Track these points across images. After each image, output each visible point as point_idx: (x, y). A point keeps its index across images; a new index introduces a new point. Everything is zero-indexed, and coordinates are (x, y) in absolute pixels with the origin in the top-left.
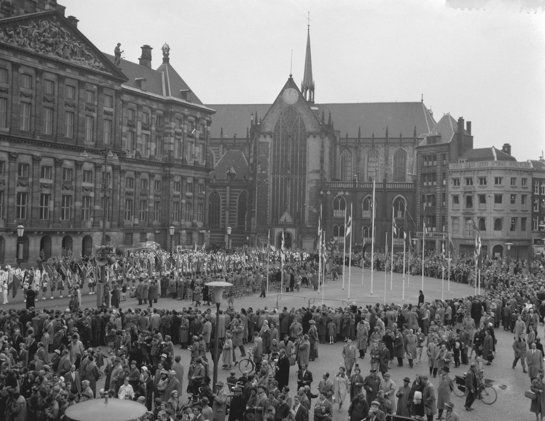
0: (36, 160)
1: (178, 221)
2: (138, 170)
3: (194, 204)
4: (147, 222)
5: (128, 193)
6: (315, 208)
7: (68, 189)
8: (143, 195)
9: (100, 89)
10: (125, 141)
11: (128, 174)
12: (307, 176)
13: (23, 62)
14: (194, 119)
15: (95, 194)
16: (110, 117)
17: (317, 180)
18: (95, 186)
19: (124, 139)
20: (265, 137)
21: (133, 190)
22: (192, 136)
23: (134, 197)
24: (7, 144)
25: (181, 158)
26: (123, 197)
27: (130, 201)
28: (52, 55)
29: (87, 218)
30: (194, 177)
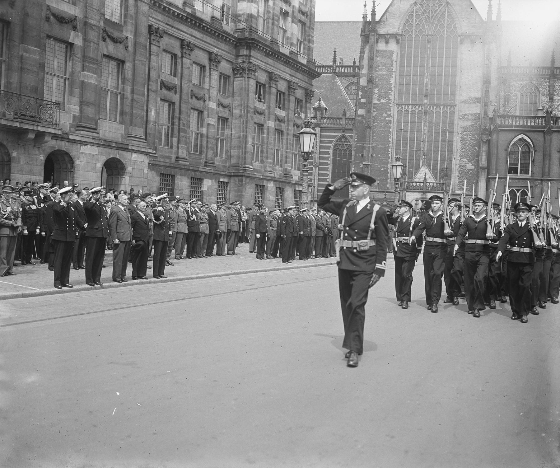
1: (262, 162)
2: (188, 38)
3: (288, 134)
4: (204, 155)
6: (470, 161)
11: (166, 40)
12: (457, 108)
15: (85, 40)
17: (475, 114)
18: (86, 17)
20: (387, 42)
21: (176, 81)
23: (178, 96)
25: (269, 38)
26: (156, 91)
30: (289, 82)
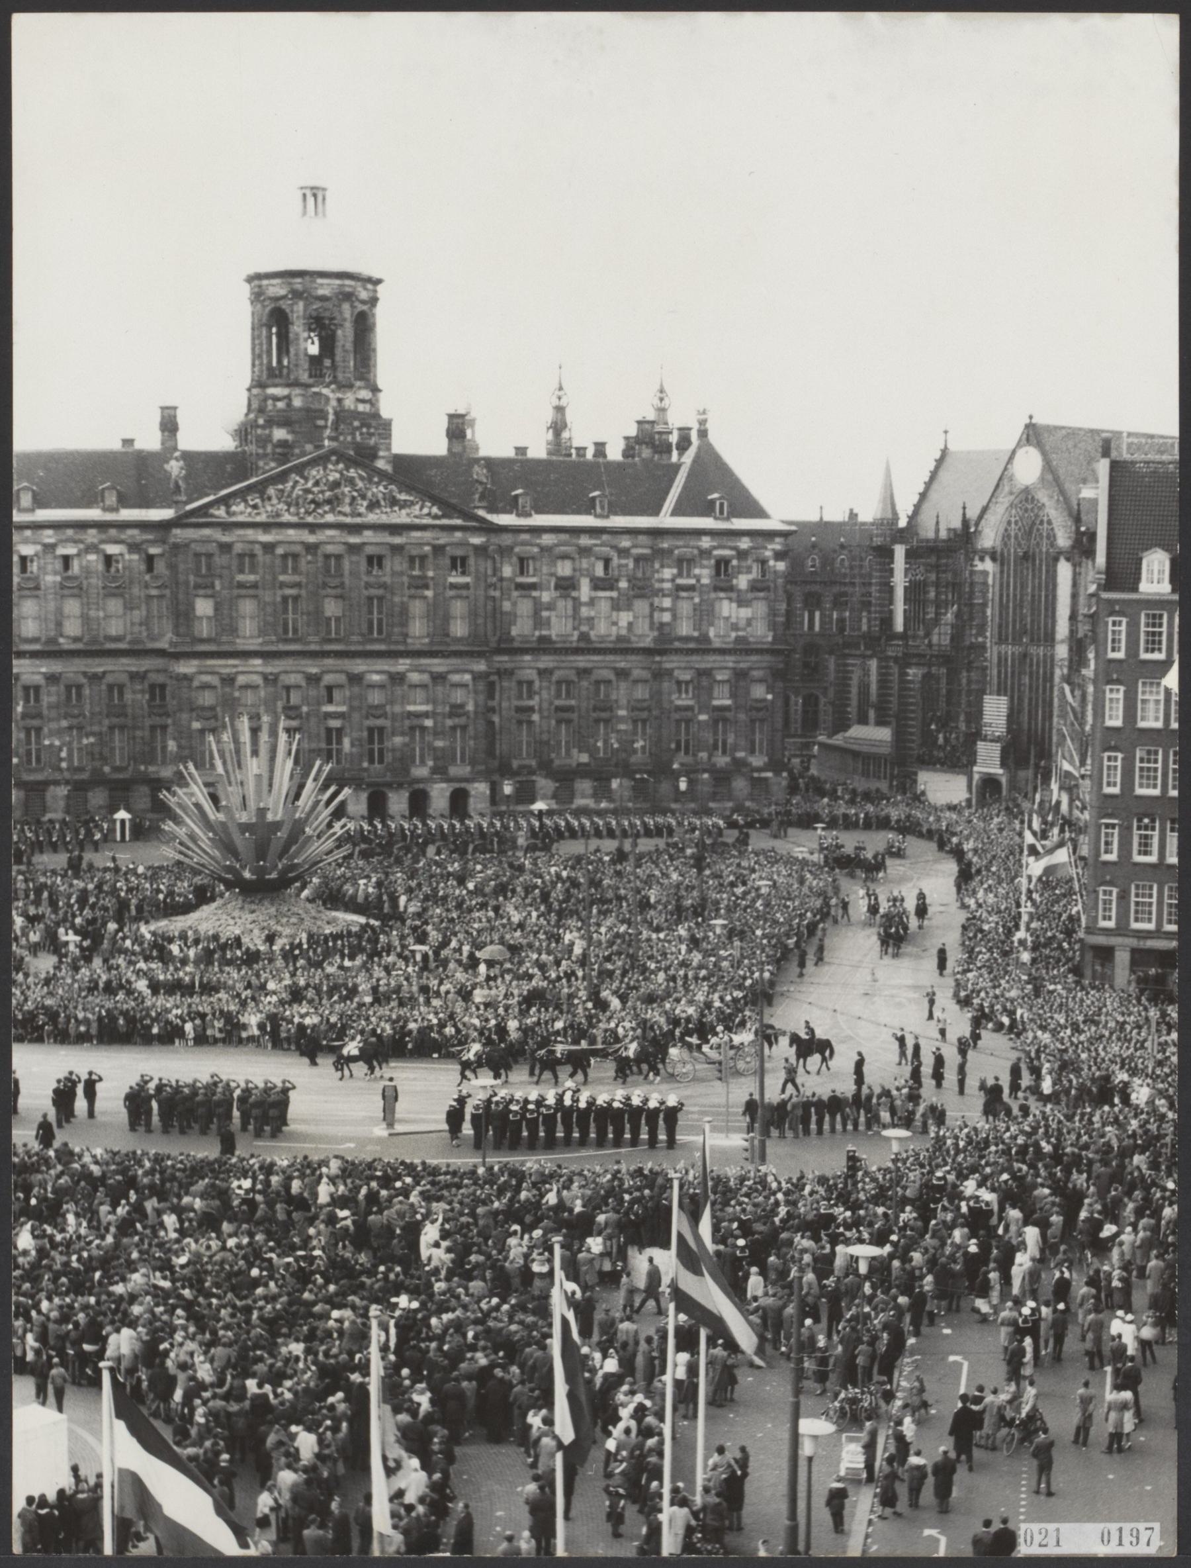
0: (313, 680)
2: (581, 665)
5: (559, 709)
7: (378, 717)
8: (603, 710)
9: (438, 550)
10: (549, 618)
13: (280, 538)
14: (733, 553)
16: (464, 593)
19: (545, 614)
21: (573, 702)
22: (731, 589)
24: (258, 662)
26: (548, 717)
27: (569, 722)
28: (330, 518)
29: (423, 763)
